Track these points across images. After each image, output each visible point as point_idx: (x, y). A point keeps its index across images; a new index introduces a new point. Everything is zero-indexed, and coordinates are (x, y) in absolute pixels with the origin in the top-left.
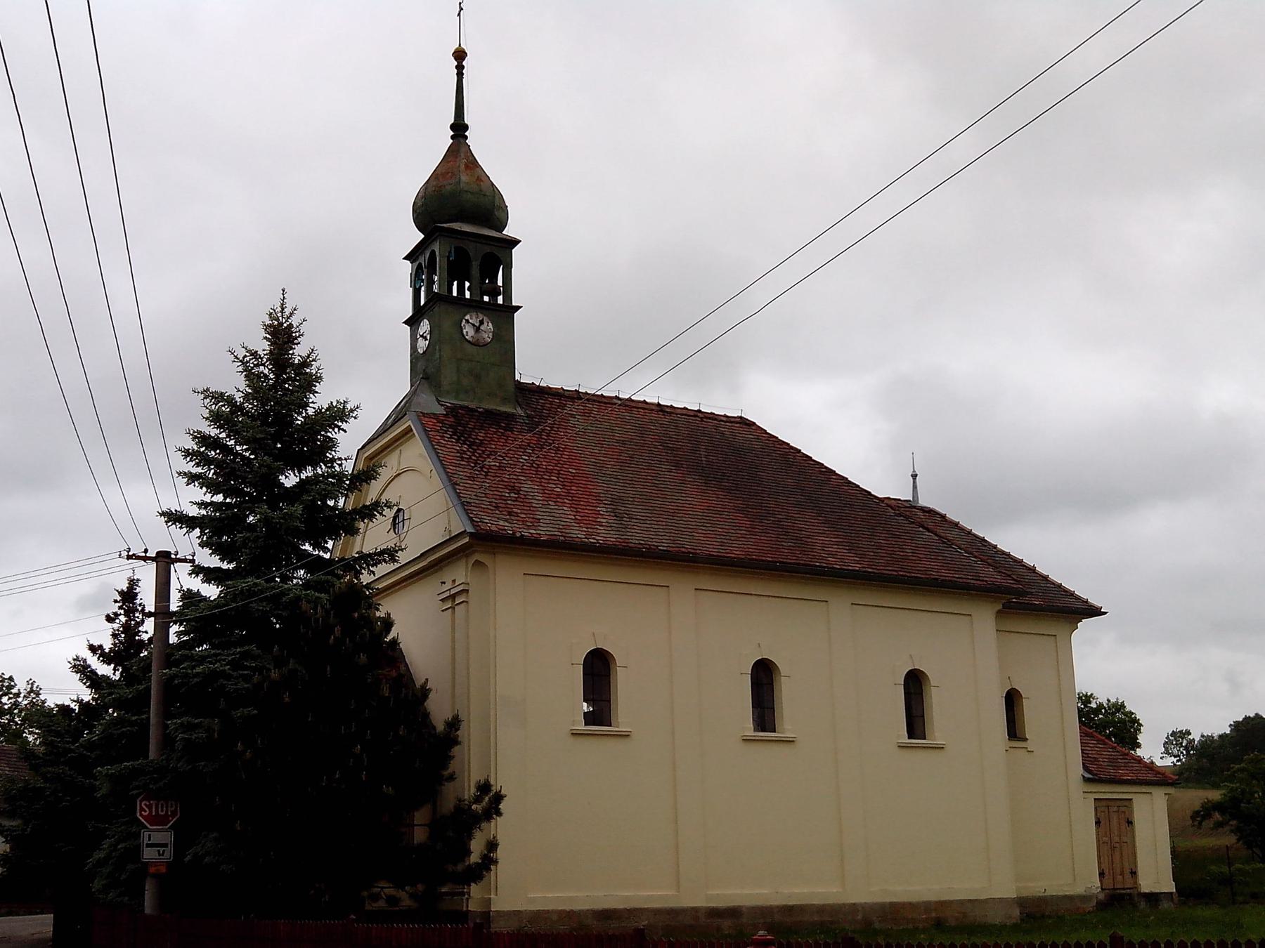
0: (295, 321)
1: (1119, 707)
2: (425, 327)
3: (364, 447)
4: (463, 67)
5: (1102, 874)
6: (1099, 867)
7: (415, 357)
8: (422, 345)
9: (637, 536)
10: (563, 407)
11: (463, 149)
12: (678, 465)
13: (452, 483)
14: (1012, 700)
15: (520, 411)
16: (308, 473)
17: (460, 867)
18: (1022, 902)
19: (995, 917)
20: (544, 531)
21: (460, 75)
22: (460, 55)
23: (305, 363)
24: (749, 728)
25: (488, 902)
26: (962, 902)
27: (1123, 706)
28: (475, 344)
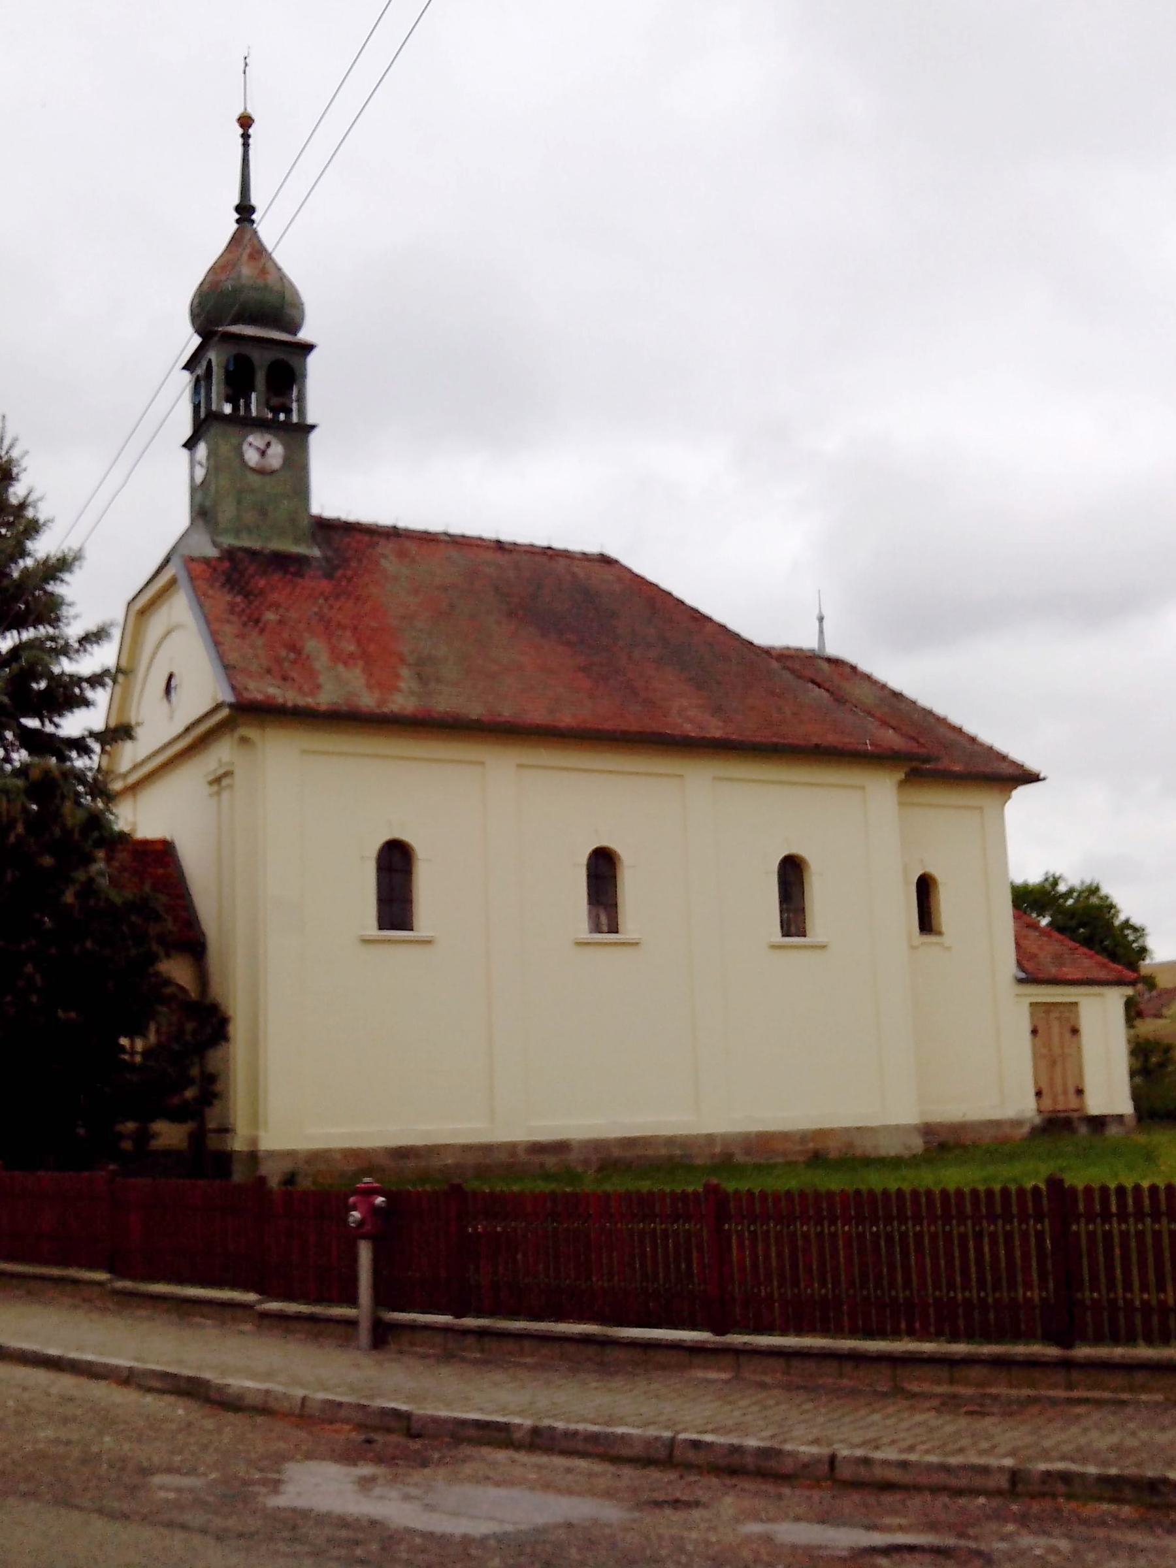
0: (15, 454)
1: (1094, 890)
2: (202, 449)
3: (134, 599)
4: (249, 136)
5: (1039, 1094)
6: (1036, 1082)
7: (194, 489)
8: (200, 474)
9: (444, 703)
10: (374, 545)
11: (248, 236)
12: (511, 614)
13: (216, 641)
14: (925, 887)
15: (316, 552)
16: (28, 634)
17: (176, 1100)
18: (927, 1130)
19: (890, 1148)
20: (325, 699)
21: (246, 145)
22: (245, 122)
23: (23, 506)
24: (370, 925)
25: (254, 1141)
26: (847, 1130)
27: (1097, 889)
28: (261, 472)
